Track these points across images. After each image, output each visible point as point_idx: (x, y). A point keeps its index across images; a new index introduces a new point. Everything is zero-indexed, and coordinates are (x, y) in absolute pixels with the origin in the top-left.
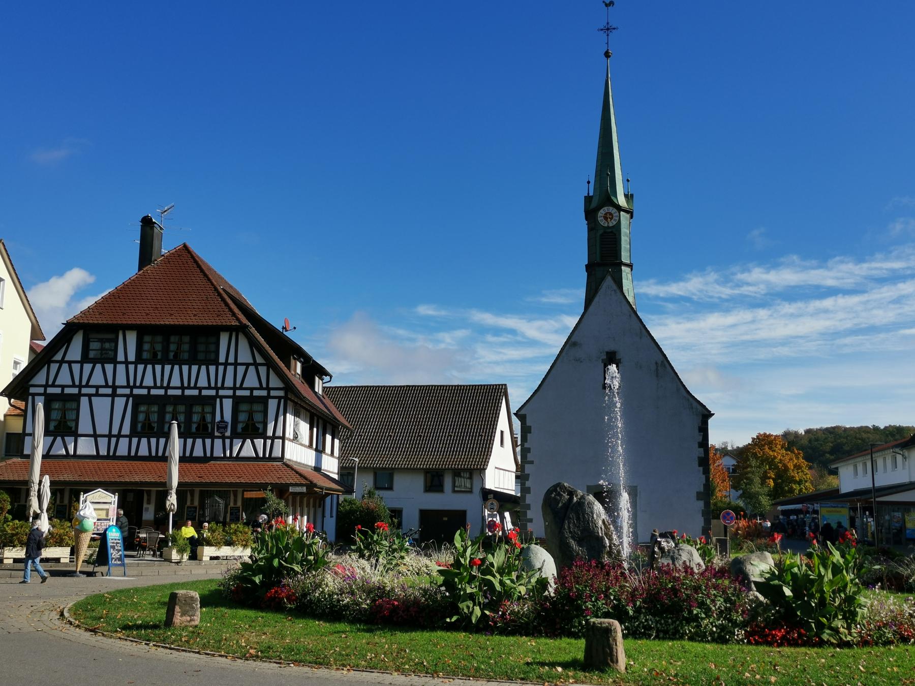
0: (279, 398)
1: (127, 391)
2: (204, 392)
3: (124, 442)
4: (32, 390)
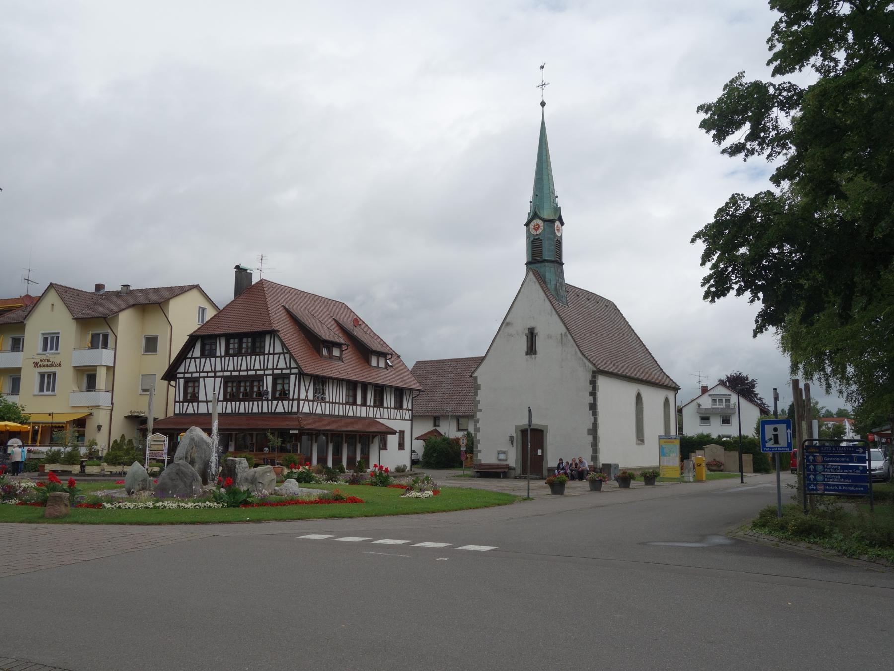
1: (221, 374)
2: (258, 373)
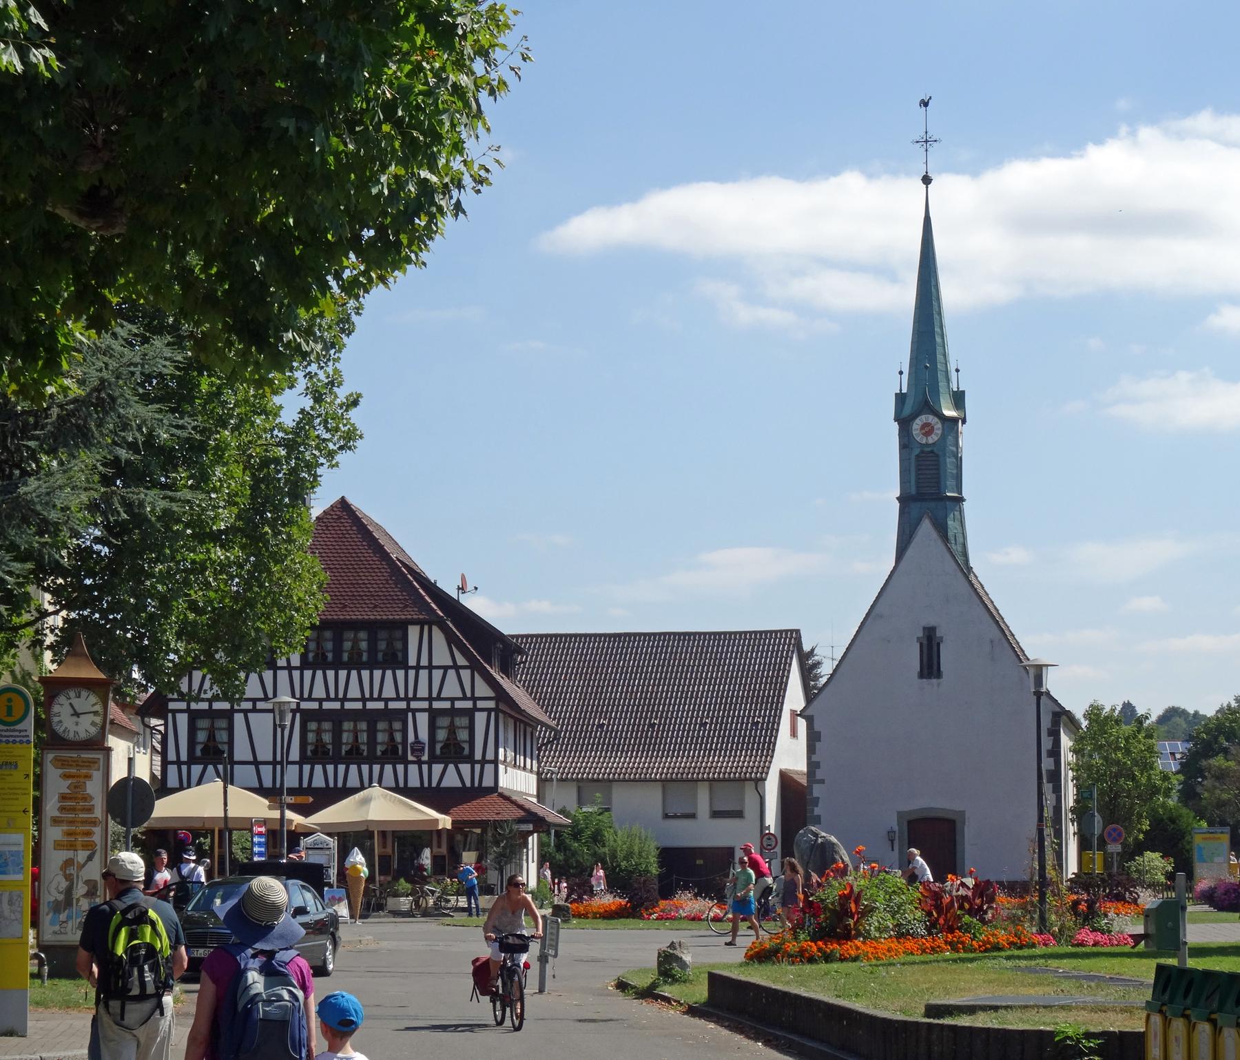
0: (489, 710)
2: (392, 705)
3: (292, 771)
4: (172, 706)
